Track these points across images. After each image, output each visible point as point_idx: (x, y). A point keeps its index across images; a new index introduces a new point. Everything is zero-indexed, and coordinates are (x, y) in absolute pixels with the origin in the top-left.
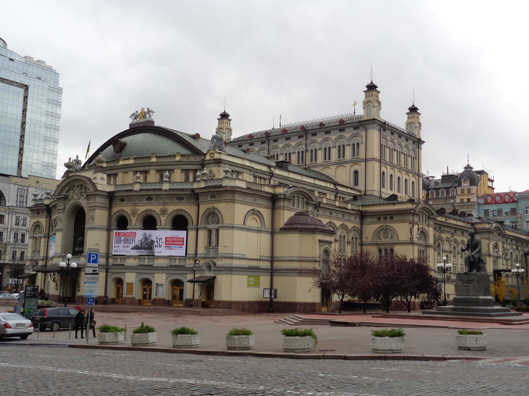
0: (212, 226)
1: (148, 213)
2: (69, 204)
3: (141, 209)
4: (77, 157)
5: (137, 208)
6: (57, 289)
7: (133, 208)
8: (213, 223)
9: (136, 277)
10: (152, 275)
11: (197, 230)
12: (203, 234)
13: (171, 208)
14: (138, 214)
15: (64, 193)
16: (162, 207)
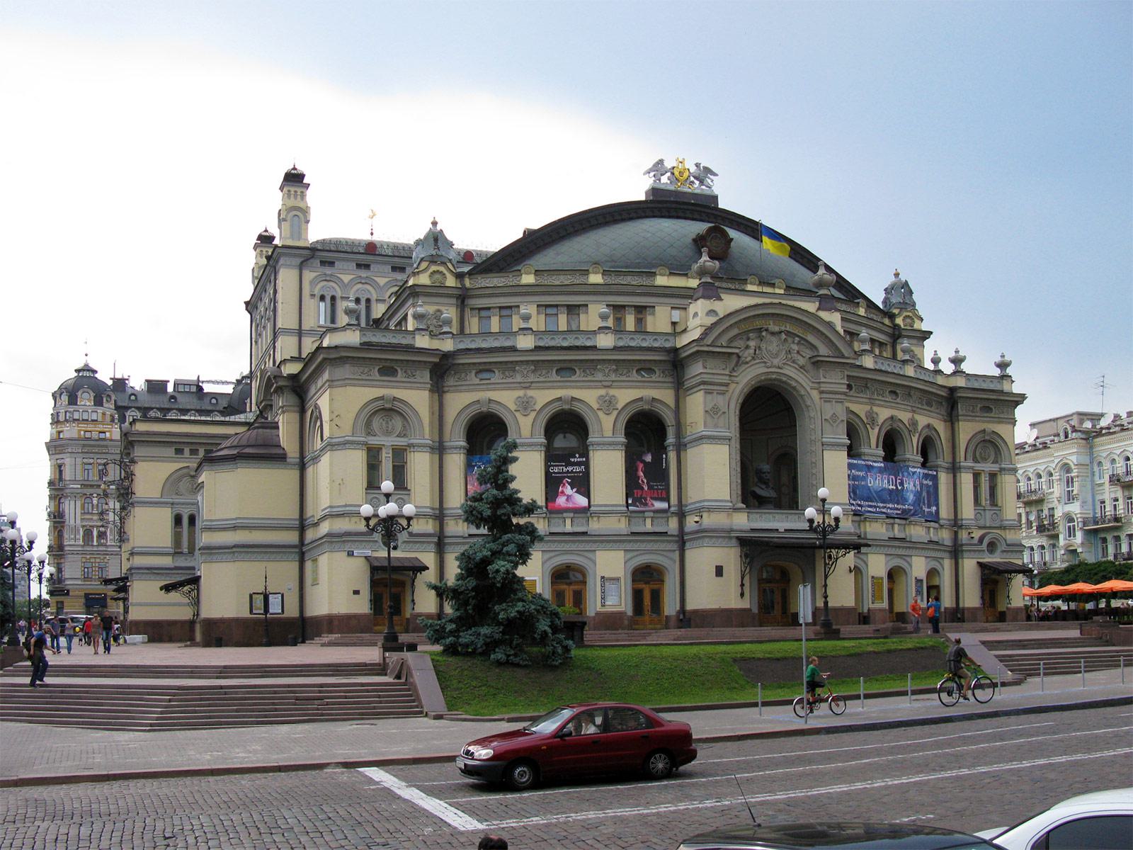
0: (988, 467)
1: (895, 426)
2: (747, 377)
3: (883, 414)
4: (435, 223)
5: (875, 409)
6: (742, 595)
7: (868, 408)
8: (985, 459)
9: (886, 564)
10: (908, 559)
11: (954, 469)
12: (966, 480)
13: (922, 420)
14: (880, 421)
15: (724, 341)
16: (909, 415)
